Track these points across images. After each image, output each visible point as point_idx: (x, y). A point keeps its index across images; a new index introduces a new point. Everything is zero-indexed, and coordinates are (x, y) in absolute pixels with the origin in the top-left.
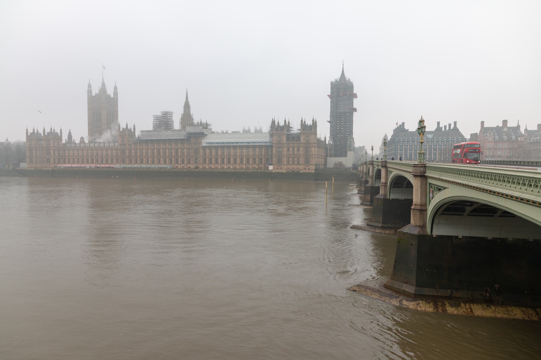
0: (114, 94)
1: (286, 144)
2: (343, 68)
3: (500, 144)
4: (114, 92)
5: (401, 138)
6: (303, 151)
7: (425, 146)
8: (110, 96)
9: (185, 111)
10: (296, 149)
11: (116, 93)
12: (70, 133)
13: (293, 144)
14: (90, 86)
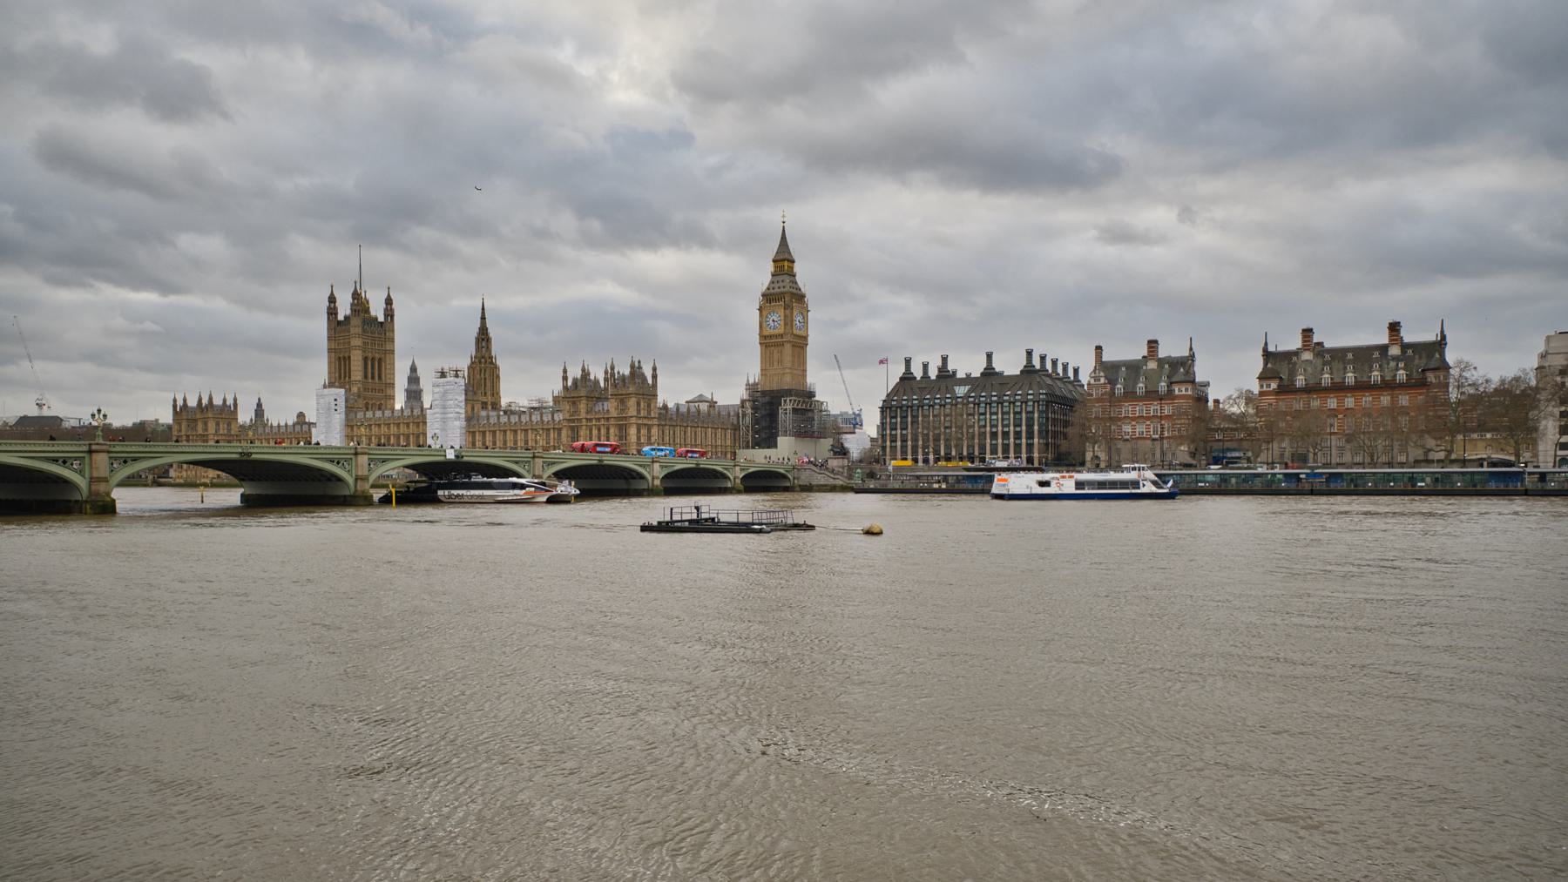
0: (386, 316)
1: (584, 420)
2: (784, 230)
3: (1126, 404)
4: (386, 310)
5: (896, 398)
6: (616, 435)
7: (947, 415)
8: (376, 319)
9: (478, 348)
10: (603, 431)
11: (389, 313)
12: (259, 405)
13: (599, 419)
14: (332, 299)
